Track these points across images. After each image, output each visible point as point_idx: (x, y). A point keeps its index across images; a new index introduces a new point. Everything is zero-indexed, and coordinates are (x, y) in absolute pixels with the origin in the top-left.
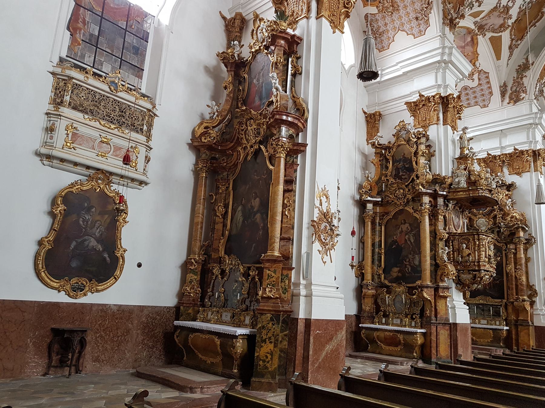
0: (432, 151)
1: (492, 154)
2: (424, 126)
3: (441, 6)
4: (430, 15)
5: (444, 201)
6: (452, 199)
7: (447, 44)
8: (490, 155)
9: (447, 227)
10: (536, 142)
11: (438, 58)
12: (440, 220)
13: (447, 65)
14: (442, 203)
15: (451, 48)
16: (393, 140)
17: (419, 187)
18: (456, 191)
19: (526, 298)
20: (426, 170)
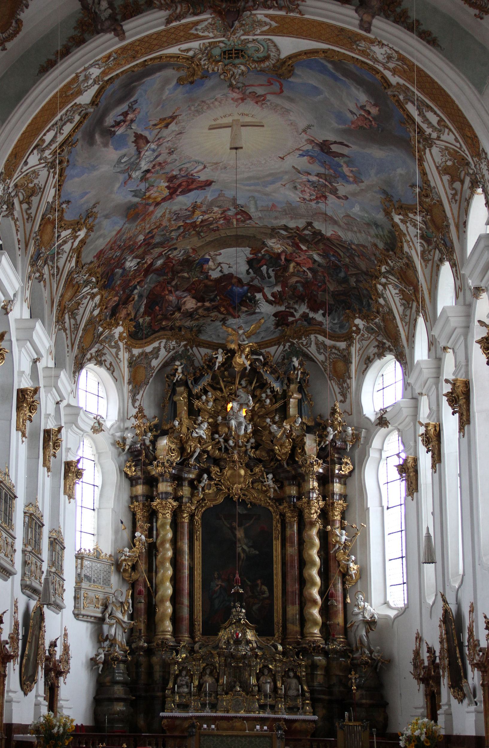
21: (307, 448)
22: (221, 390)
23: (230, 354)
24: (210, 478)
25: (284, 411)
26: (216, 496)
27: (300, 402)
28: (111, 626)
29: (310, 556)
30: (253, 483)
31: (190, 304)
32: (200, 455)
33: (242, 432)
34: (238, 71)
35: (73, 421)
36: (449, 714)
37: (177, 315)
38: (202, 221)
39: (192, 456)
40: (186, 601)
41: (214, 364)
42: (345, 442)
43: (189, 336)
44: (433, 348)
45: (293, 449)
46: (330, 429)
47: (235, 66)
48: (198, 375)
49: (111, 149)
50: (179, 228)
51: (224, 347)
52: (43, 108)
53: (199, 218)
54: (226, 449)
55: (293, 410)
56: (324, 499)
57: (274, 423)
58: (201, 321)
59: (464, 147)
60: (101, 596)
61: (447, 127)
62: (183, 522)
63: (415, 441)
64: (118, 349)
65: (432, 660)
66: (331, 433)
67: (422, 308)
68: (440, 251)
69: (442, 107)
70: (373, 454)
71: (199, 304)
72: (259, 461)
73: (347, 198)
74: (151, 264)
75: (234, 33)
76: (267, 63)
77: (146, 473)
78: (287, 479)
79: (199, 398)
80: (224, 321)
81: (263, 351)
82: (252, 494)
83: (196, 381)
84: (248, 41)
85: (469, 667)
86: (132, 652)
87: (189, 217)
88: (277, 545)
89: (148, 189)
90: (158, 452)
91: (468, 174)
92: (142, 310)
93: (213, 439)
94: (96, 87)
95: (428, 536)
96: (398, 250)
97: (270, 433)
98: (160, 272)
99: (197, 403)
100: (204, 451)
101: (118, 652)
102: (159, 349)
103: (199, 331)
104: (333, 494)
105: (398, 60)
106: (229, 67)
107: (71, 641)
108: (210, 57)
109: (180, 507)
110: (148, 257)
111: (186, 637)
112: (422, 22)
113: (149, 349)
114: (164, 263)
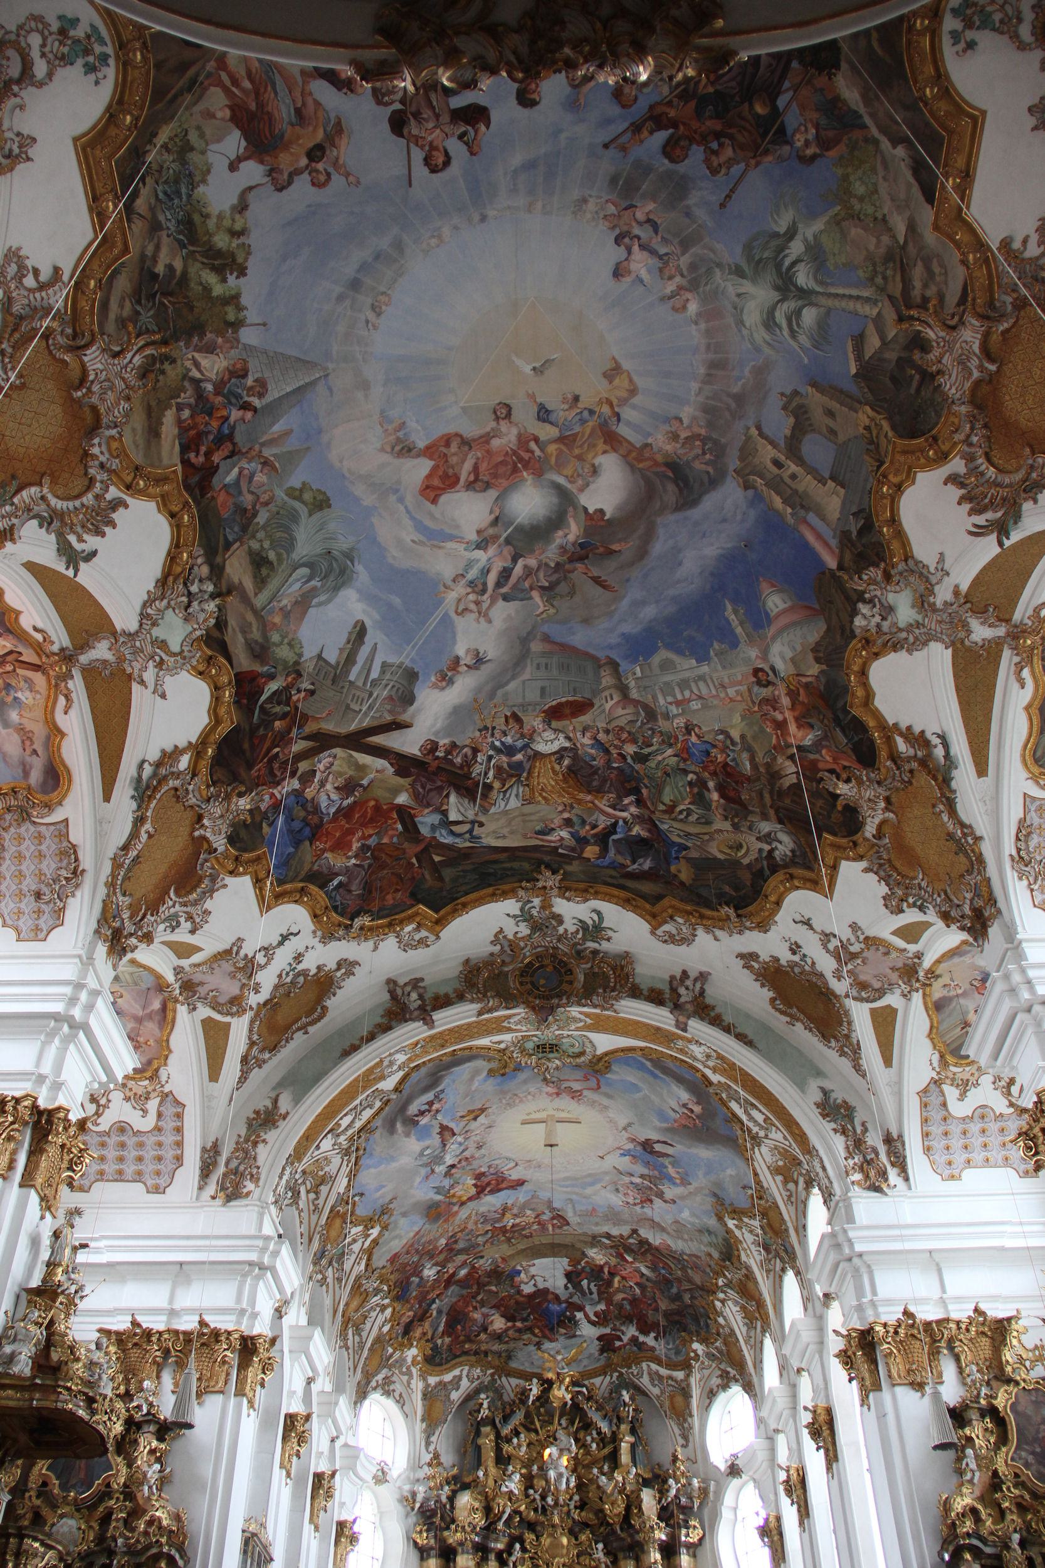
3: (102, 892)
4: (70, 900)
7: (92, 982)
8: (139, 1325)
10: (255, 1316)
11: (58, 1007)
13: (74, 1031)
15: (95, 993)
21: (644, 1506)
23: (547, 1385)
24: (524, 1549)
25: (613, 1459)
27: (633, 1447)
30: (578, 1556)
31: (499, 1323)
32: (510, 1517)
33: (564, 1486)
34: (552, 1065)
37: (483, 1336)
39: (500, 1519)
41: (528, 1397)
42: (691, 1498)
43: (497, 1363)
44: (785, 1373)
45: (628, 1509)
47: (549, 1060)
48: (508, 1411)
51: (539, 1377)
53: (509, 1221)
55: (625, 1458)
58: (512, 1345)
66: (673, 1487)
67: (766, 1327)
69: (766, 1105)
70: (726, 1514)
72: (585, 1525)
74: (453, 1275)
75: (548, 1027)
77: (442, 1541)
78: (622, 1549)
79: (509, 1441)
80: (538, 1345)
83: (506, 1419)
84: (561, 1037)
89: (452, 1186)
91: (801, 1174)
92: (441, 1329)
93: (527, 1496)
94: (401, 1074)
96: (734, 1260)
97: (599, 1487)
98: (464, 1283)
99: (507, 1448)
100: (516, 1512)
102: (460, 1378)
103: (509, 1357)
108: (523, 1050)
113: (448, 1377)
114: (469, 1274)
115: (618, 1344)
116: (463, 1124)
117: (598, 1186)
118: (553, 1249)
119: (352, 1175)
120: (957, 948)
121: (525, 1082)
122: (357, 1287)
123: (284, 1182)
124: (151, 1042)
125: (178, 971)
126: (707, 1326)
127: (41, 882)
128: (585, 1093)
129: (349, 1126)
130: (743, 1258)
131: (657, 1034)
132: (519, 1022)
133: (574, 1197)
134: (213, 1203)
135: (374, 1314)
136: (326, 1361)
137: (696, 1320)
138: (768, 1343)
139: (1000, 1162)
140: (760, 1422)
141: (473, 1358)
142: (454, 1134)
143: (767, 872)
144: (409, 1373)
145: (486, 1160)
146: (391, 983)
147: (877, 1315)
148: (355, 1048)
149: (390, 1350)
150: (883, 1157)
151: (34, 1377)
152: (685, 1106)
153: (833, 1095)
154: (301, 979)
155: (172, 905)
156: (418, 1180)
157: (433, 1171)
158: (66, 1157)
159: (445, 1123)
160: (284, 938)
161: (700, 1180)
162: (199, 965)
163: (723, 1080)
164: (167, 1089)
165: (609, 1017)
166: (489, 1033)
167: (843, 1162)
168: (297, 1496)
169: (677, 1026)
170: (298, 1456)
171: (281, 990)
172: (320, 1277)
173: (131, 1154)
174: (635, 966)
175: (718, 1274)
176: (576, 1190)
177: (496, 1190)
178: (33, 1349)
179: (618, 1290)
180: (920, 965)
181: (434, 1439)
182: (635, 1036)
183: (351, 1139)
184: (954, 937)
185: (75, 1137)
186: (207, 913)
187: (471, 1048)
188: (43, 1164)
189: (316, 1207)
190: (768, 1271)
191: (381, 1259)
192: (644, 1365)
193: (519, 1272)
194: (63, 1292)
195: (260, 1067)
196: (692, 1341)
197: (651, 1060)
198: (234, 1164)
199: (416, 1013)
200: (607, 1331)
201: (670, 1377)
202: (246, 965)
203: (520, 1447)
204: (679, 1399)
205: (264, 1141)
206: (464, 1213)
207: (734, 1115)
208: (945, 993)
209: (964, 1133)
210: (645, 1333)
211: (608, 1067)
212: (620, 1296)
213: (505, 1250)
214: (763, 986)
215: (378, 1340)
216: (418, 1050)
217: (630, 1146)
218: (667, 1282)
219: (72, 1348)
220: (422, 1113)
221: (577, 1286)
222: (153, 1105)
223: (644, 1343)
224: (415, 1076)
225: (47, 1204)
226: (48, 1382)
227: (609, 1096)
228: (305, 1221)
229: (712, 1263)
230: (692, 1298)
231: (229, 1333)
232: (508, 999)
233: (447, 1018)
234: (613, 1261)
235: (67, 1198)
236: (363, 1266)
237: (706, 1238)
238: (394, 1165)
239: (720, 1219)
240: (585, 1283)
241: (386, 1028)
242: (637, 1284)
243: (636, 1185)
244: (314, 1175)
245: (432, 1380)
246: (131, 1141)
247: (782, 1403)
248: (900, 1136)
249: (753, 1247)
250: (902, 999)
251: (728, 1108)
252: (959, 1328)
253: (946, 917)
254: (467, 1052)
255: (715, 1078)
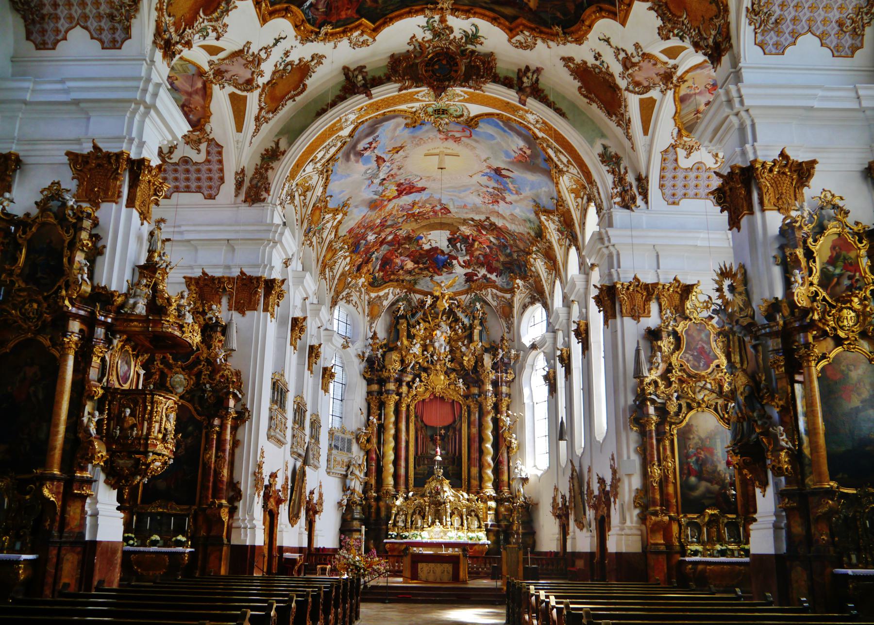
0: (100, 244)
1: (210, 274)
2: (94, 201)
3: (154, 14)
4: (133, 21)
5: (106, 334)
6: (122, 333)
9: (105, 380)
12: (93, 364)
14: (102, 337)
16: (35, 212)
17: (64, 302)
18: (129, 318)
19: (224, 502)
20: (82, 275)
21: (485, 362)
22: (429, 322)
23: (436, 299)
24: (421, 381)
26: (425, 392)
27: (481, 332)
28: (352, 480)
29: (487, 435)
30: (449, 385)
31: (410, 265)
32: (414, 365)
33: (443, 351)
35: (330, 339)
36: (574, 538)
37: (401, 272)
38: (419, 213)
39: (409, 366)
40: (403, 463)
42: (509, 359)
45: (476, 363)
46: (500, 350)
47: (442, 119)
49: (361, 163)
50: (404, 216)
51: (431, 294)
52: (318, 137)
54: (432, 362)
55: (476, 337)
56: (496, 397)
57: (464, 345)
58: (417, 277)
59: (583, 178)
60: (346, 460)
61: (572, 165)
62: (402, 411)
63: (555, 360)
64: (361, 293)
65: (564, 504)
68: (569, 239)
69: (569, 153)
71: (416, 266)
72: (453, 370)
73: (511, 203)
74: (385, 238)
75: (441, 99)
76: (462, 119)
78: (471, 382)
79: (414, 327)
80: (432, 277)
81: (457, 298)
82: (449, 392)
83: (413, 315)
85: (587, 508)
86: (366, 499)
87: (410, 210)
88: (465, 427)
90: (386, 363)
92: (378, 268)
93: (423, 355)
94: (353, 126)
95: (562, 422)
97: (461, 352)
98: (390, 243)
99: (413, 331)
101: (356, 498)
102: (388, 294)
103: (415, 283)
104: (502, 393)
105: (543, 123)
106: (438, 119)
107: (323, 491)
108: (426, 113)
109: (400, 400)
110: (382, 234)
111: (402, 488)
112: (556, 103)
113: (381, 293)
114: (393, 238)
115: (475, 278)
116: (390, 155)
117: (468, 192)
118: (441, 226)
119: (325, 186)
120: (701, 64)
121: (427, 131)
122: (330, 247)
123: (285, 192)
124: (199, 108)
125: (211, 63)
126: (525, 271)
127: (112, 7)
128: (463, 139)
129: (322, 157)
130: (548, 237)
131: (507, 106)
132: (424, 96)
133: (453, 198)
134: (243, 205)
135: (340, 261)
136: (313, 289)
137: (519, 267)
138: (558, 282)
139: (704, 196)
140: (549, 324)
141: (395, 284)
142: (384, 161)
143: (585, 5)
144: (360, 291)
145: (404, 176)
146: (346, 70)
147: (619, 279)
148: (323, 111)
149: (350, 279)
150: (634, 189)
151: (147, 316)
152: (521, 149)
153: (610, 150)
154: (289, 67)
155: (202, 21)
156: (364, 187)
157: (372, 182)
158: (152, 188)
159: (379, 155)
160: (277, 41)
161: (527, 192)
162: (224, 59)
163: (545, 136)
164: (211, 137)
165: (478, 94)
166: (406, 102)
167: (610, 191)
168: (300, 357)
169: (520, 102)
170: (300, 339)
171: (277, 75)
172: (309, 242)
173: (193, 176)
174: (497, 61)
175: (533, 244)
176: (455, 194)
177: (409, 193)
178: (146, 301)
179: (477, 249)
180: (675, 73)
181: (374, 325)
182: (494, 107)
183: (323, 165)
184: (700, 58)
185: (156, 176)
186: (225, 25)
187: (394, 111)
188: (138, 194)
189: (305, 204)
190: (561, 245)
191: (343, 231)
192: (489, 290)
193: (422, 238)
194: (159, 267)
195: (267, 122)
196: (516, 279)
197: (503, 121)
198: (255, 182)
199: (361, 89)
200: (470, 271)
201: (504, 297)
202: (253, 60)
203: (420, 330)
204: (507, 309)
205: (272, 168)
206: (391, 205)
207: (550, 157)
208: (688, 91)
209: (685, 178)
210: (491, 272)
211: (477, 124)
212: (478, 253)
213: (414, 225)
214: (575, 78)
215: (343, 274)
216: (362, 112)
217: (488, 171)
218: (505, 246)
219: (169, 299)
220: (365, 149)
221: (454, 246)
222: (203, 146)
223: (489, 278)
224: (361, 128)
225: (144, 216)
226: (156, 318)
227: (477, 141)
228: (299, 212)
229: (531, 238)
230: (518, 256)
231: (258, 279)
232: (418, 81)
233: (382, 92)
234: (475, 233)
235: (156, 213)
236: (333, 236)
237: (528, 225)
238: (349, 179)
239: (537, 214)
240: (458, 245)
241: (341, 98)
242: (487, 246)
243: (491, 193)
244: (302, 186)
245: (373, 295)
246: (192, 169)
247: (563, 317)
248: (647, 177)
249: (554, 232)
250: (661, 94)
251: (546, 153)
252: (664, 288)
253: (697, 46)
254: (392, 113)
255: (540, 134)
